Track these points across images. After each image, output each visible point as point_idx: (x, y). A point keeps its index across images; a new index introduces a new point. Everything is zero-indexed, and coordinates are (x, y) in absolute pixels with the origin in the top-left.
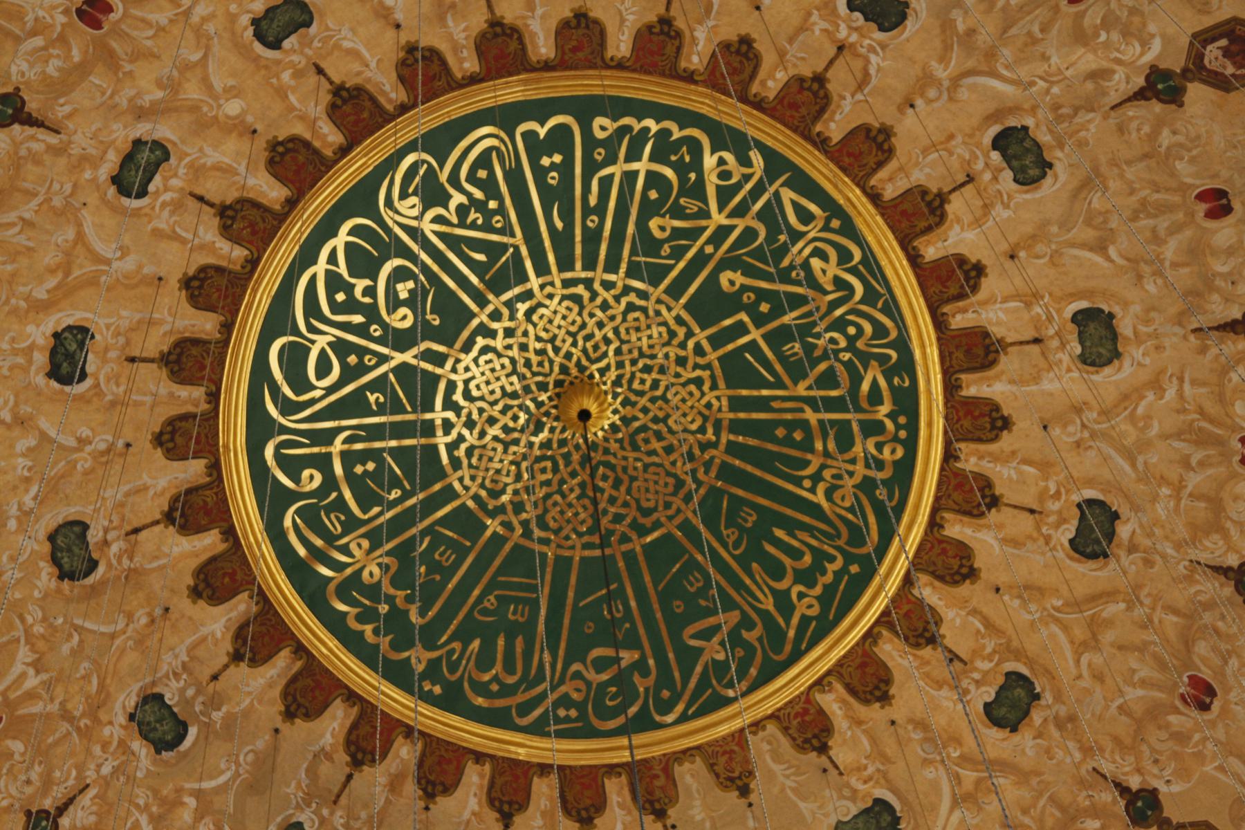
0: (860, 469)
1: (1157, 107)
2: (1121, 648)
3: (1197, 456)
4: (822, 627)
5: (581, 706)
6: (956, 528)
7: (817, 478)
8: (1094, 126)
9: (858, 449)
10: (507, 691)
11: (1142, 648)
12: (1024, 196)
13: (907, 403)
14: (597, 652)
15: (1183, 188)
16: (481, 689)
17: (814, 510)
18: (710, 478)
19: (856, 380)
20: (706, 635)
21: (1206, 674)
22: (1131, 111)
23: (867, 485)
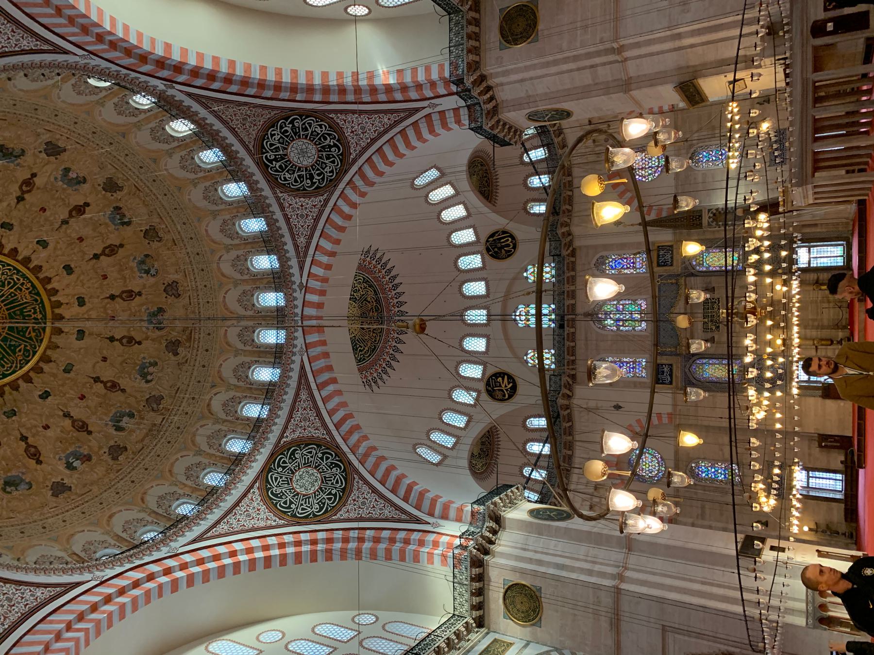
0: (27, 291)
1: (22, 203)
2: (88, 281)
3: (73, 247)
4: (45, 317)
5: (24, 359)
6: (49, 287)
7: (22, 299)
8: (15, 213)
9: (23, 289)
10: (11, 367)
11: (91, 279)
12: (12, 232)
13: (24, 277)
14: (18, 350)
15: (36, 212)
16: (7, 370)
17: (26, 303)
18: (6, 313)
19: (13, 280)
20: (30, 333)
21: (103, 274)
22: (18, 206)
23: (30, 293)
